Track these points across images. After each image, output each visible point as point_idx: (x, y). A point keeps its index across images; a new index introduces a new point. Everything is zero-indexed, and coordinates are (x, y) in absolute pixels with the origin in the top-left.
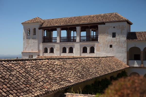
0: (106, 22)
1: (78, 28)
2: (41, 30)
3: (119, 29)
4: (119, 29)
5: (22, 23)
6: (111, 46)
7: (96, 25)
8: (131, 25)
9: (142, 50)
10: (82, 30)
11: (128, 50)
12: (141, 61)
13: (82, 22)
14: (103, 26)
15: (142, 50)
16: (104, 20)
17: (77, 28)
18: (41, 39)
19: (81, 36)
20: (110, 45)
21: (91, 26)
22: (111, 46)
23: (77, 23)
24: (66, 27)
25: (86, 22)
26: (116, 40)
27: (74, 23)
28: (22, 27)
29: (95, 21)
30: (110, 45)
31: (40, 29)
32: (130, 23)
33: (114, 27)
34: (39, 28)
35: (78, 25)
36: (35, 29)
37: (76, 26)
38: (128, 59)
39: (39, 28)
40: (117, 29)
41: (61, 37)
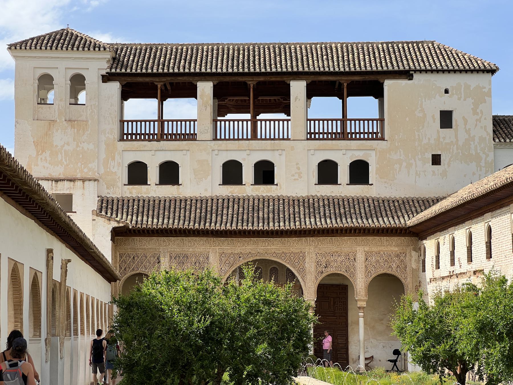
0: (415, 71)
1: (298, 88)
2: (115, 87)
3: (465, 100)
4: (465, 100)
6: (436, 160)
7: (372, 78)
13: (315, 66)
14: (403, 83)
19: (310, 120)
21: (353, 82)
22: (436, 160)
24: (147, 80)
25: (332, 66)
26: (456, 137)
28: (9, 60)
31: (107, 78)
33: (447, 91)
34: (103, 76)
35: (298, 75)
37: (285, 79)
39: (103, 76)
40: (459, 99)
41: (125, 119)
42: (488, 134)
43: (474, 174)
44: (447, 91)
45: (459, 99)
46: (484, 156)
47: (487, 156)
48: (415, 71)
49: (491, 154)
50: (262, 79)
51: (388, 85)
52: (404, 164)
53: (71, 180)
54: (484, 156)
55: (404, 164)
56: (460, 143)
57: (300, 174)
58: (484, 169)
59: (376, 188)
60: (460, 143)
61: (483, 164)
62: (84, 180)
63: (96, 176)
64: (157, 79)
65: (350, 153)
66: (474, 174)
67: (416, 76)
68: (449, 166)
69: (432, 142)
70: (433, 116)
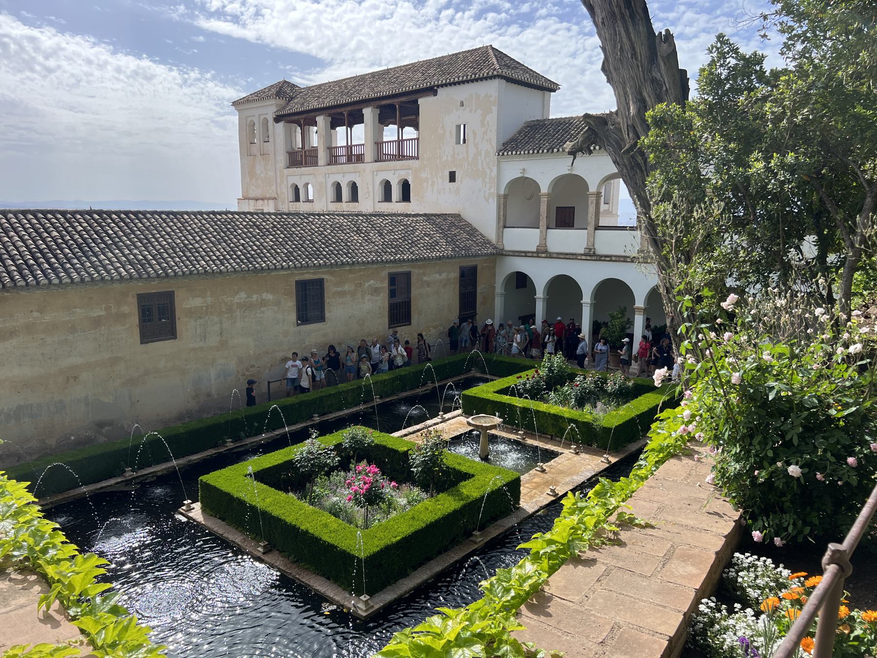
0: (438, 86)
1: (368, 113)
2: (281, 125)
5: (234, 104)
6: (452, 177)
8: (554, 91)
9: (544, 189)
10: (385, 118)
11: (502, 192)
12: (541, 232)
15: (544, 189)
16: (435, 81)
17: (364, 111)
18: (282, 159)
20: (451, 173)
22: (452, 177)
23: (366, 93)
26: (467, 152)
27: (356, 98)
29: (410, 86)
30: (451, 173)
31: (278, 119)
32: (549, 87)
33: (462, 104)
35: (367, 102)
36: (266, 121)
38: (501, 224)
42: (492, 147)
43: (480, 190)
44: (462, 104)
45: (471, 111)
46: (488, 171)
47: (491, 171)
48: (438, 86)
49: (495, 169)
50: (350, 108)
51: (424, 102)
52: (430, 182)
53: (262, 199)
54: (488, 171)
55: (430, 182)
56: (470, 159)
57: (369, 192)
58: (488, 185)
59: (413, 207)
60: (470, 159)
61: (487, 180)
62: (269, 199)
63: (275, 195)
64: (300, 117)
65: (397, 173)
66: (480, 190)
67: (440, 91)
68: (461, 181)
69: (449, 158)
70: (451, 132)
